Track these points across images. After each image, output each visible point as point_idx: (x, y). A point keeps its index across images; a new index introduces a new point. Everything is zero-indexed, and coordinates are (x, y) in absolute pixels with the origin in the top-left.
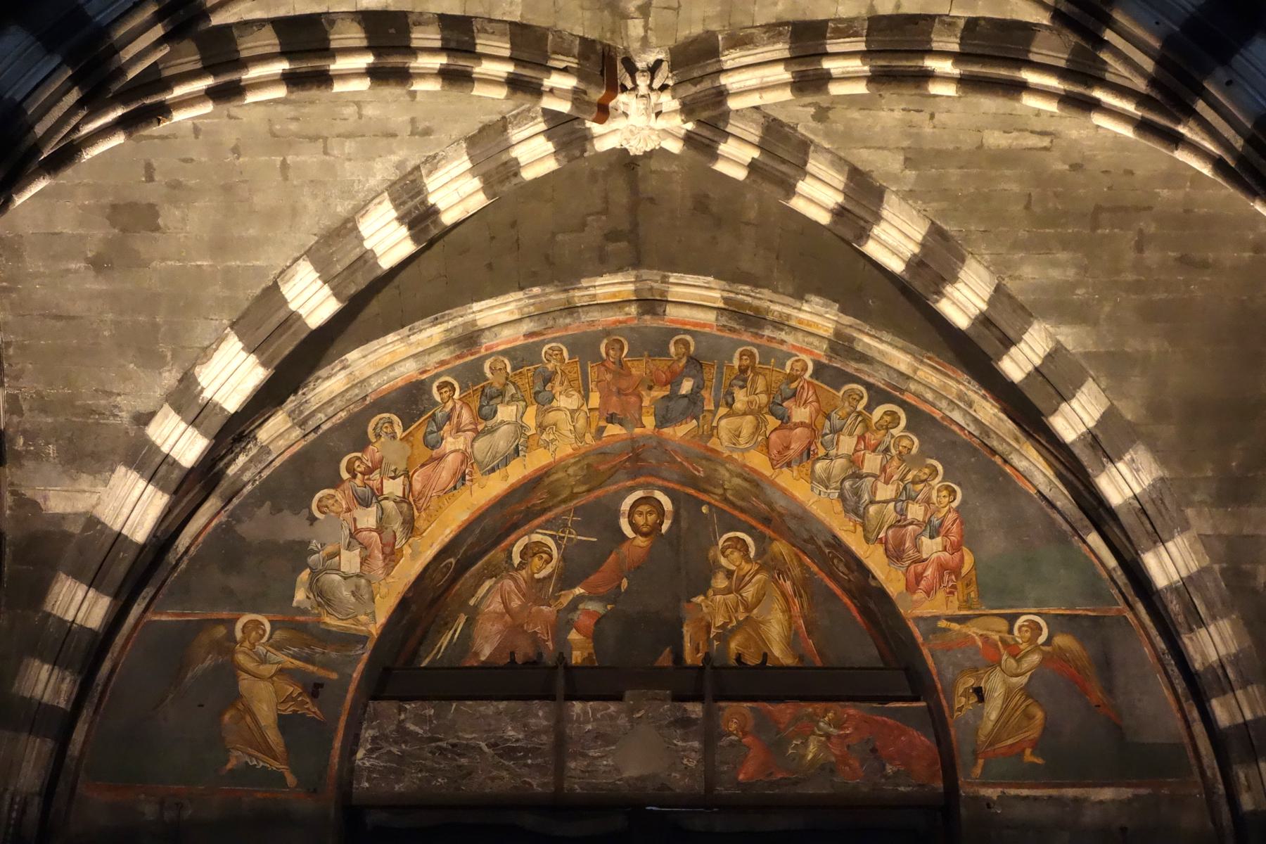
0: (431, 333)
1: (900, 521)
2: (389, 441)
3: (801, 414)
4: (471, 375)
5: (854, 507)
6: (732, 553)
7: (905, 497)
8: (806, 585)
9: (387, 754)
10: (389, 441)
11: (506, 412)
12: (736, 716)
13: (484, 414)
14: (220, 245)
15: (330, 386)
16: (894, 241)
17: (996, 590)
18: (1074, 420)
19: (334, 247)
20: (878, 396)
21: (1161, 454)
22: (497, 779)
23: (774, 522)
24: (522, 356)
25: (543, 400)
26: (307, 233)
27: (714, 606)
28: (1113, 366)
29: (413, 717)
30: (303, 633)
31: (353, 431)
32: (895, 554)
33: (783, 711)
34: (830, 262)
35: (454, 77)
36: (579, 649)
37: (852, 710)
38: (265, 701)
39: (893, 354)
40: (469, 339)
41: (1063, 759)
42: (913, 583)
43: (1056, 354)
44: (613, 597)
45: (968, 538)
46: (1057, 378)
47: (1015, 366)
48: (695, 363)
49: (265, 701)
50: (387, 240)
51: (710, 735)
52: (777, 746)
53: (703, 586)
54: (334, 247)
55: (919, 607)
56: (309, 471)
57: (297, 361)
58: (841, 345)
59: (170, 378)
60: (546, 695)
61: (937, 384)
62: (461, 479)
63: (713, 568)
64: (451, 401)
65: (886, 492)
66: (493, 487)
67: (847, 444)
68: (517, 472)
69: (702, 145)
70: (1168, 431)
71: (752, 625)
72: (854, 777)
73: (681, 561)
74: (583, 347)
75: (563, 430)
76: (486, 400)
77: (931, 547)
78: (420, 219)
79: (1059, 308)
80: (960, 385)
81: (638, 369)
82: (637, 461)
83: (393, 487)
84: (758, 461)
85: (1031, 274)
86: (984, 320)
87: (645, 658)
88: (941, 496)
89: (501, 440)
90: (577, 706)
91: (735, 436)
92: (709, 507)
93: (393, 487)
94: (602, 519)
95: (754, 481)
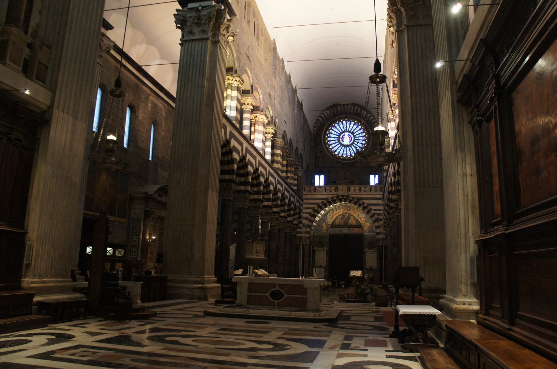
2: (331, 212)
6: (352, 218)
9: (331, 231)
10: (331, 212)
17: (366, 221)
22: (338, 232)
23: (354, 216)
27: (350, 221)
29: (333, 229)
30: (326, 224)
38: (325, 228)
41: (370, 232)
49: (325, 228)
55: (362, 223)
64: (335, 209)
66: (337, 215)
72: (358, 232)
73: (348, 218)
75: (341, 211)
76: (337, 210)
87: (346, 225)
91: (351, 212)
92: (350, 215)
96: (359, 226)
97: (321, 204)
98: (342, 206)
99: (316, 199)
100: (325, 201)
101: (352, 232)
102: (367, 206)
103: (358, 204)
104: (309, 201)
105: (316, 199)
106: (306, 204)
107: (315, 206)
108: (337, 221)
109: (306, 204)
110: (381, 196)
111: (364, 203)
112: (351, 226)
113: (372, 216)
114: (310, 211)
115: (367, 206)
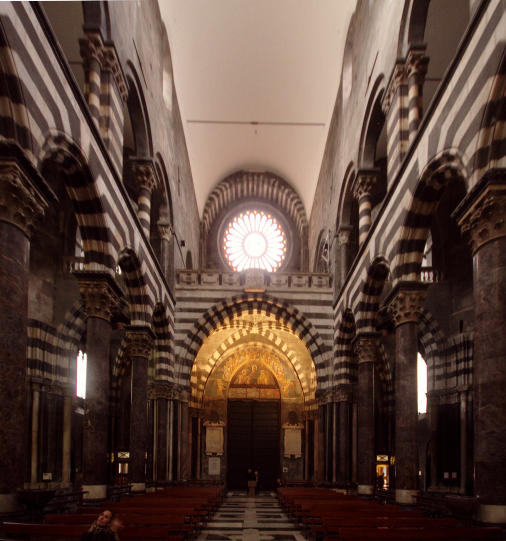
0: (235, 348)
1: (278, 370)
2: (231, 360)
3: (269, 358)
4: (238, 353)
5: (273, 369)
6: (262, 372)
7: (278, 367)
8: (269, 376)
10: (231, 360)
11: (242, 357)
12: (262, 390)
13: (240, 358)
14: (215, 341)
15: (225, 354)
16: (278, 342)
18: (294, 361)
19: (226, 342)
20: (276, 356)
21: (301, 365)
24: (243, 351)
25: (245, 356)
26: (223, 340)
28: (298, 355)
31: (227, 359)
32: (277, 373)
33: (266, 390)
34: (272, 343)
35: (238, 327)
36: (248, 383)
37: (272, 390)
39: (277, 351)
40: (238, 349)
42: (278, 377)
43: (292, 354)
44: (251, 377)
45: (284, 372)
46: (292, 357)
47: (289, 355)
48: (259, 352)
50: (231, 342)
51: (260, 392)
52: (266, 393)
53: (259, 376)
54: (226, 342)
55: (279, 379)
56: (223, 364)
57: (222, 353)
58: (273, 351)
59: (211, 355)
60: (245, 387)
61: (281, 355)
62: (237, 365)
63: (260, 374)
64: (236, 356)
65: (276, 367)
67: (273, 361)
68: (243, 364)
69: (260, 332)
70: (302, 362)
71: (264, 380)
73: (257, 374)
74: (249, 350)
75: (246, 359)
76: (240, 356)
77: (280, 373)
78: (234, 339)
79: (293, 349)
80: (284, 355)
81: (254, 353)
82: (254, 363)
83: (231, 366)
84: (265, 363)
85: (290, 345)
86: (286, 351)
88: (281, 367)
89: (241, 361)
90: (248, 389)
91: (263, 360)
92: (260, 367)
93: (231, 366)
94: (250, 368)
95: (264, 366)
96: (275, 385)
97: (212, 313)
98: (249, 350)
99: (201, 300)
100: (220, 307)
101: (263, 396)
102: (303, 318)
103: (284, 314)
104: (187, 305)
105: (201, 300)
106: (181, 310)
107: (199, 316)
108: (240, 377)
109: (181, 310)
110: (331, 298)
111: (296, 311)
112: (261, 386)
113: (313, 340)
114: (189, 326)
115: (303, 318)
